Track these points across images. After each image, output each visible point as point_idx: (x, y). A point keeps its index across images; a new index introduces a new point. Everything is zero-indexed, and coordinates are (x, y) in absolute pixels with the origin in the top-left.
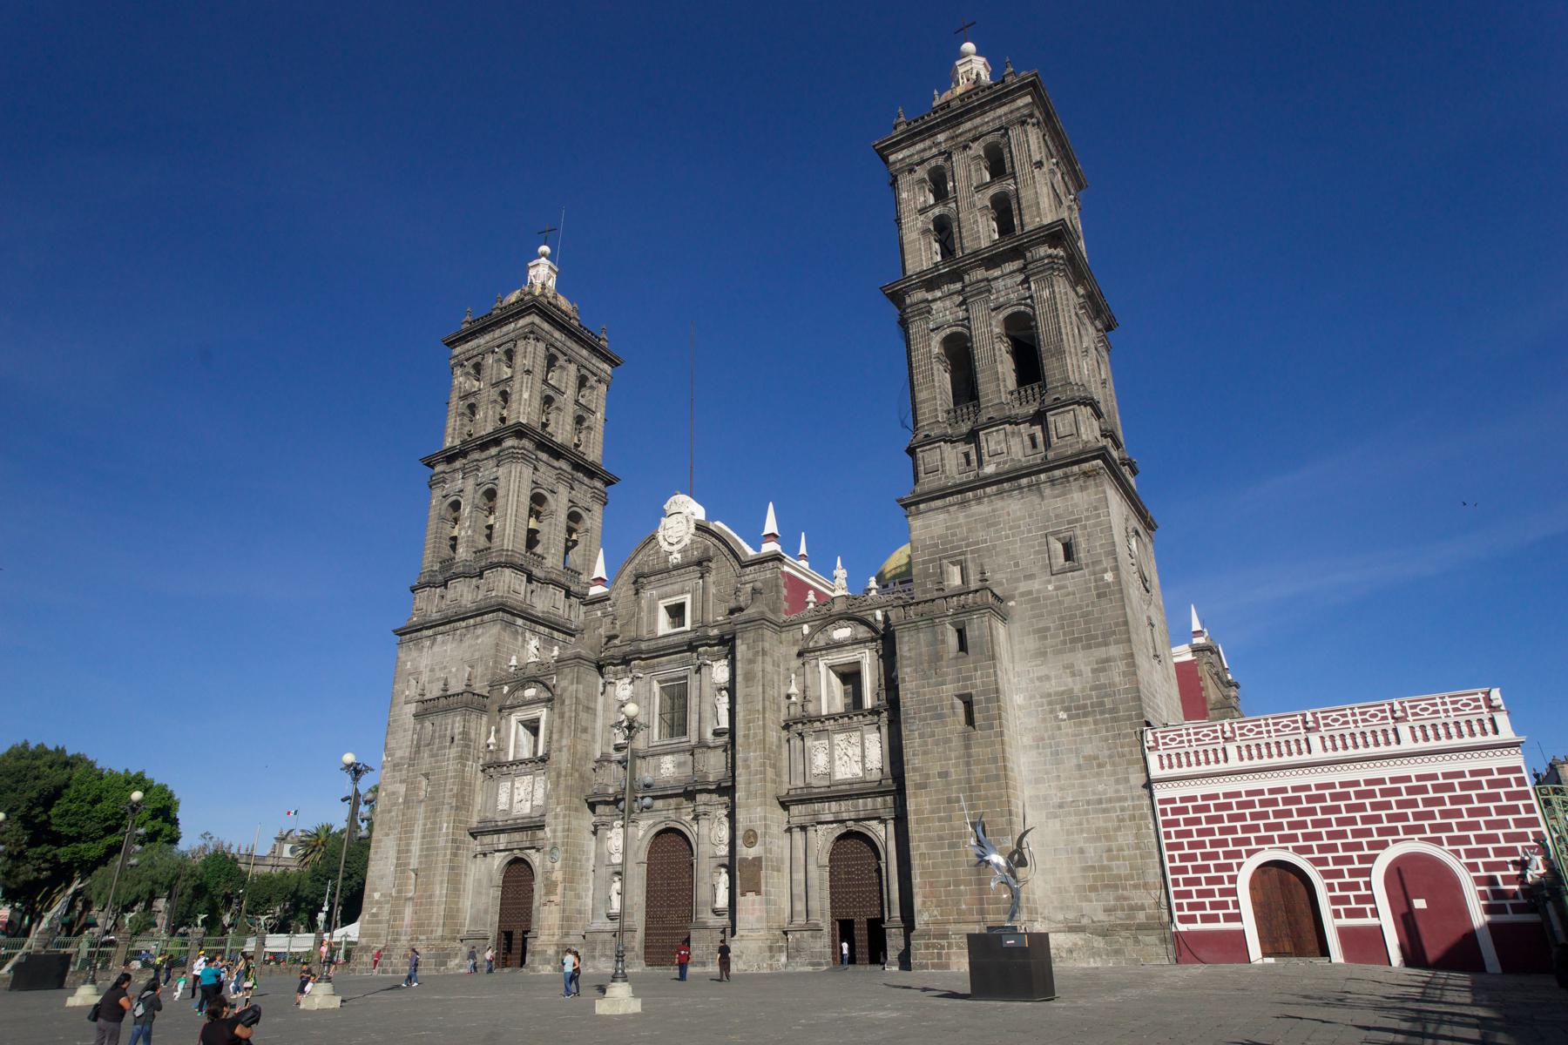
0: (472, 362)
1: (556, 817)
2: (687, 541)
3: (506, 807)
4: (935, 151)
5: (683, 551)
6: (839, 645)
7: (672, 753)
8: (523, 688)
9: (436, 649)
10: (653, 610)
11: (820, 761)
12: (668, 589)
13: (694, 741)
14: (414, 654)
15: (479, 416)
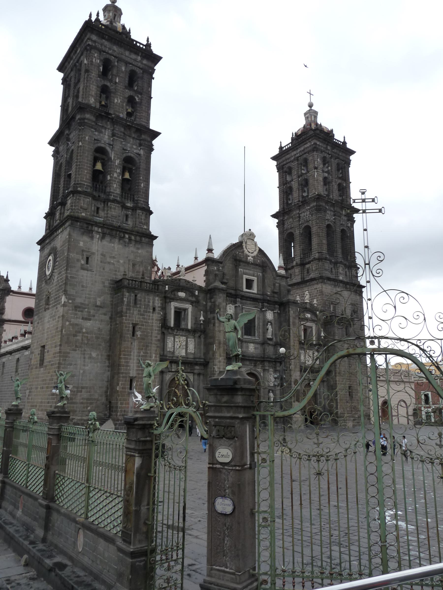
0: (108, 56)
1: (220, 362)
2: (255, 253)
3: (172, 350)
4: (327, 151)
5: (253, 257)
6: (307, 319)
7: (253, 343)
8: (179, 291)
9: (105, 242)
10: (242, 278)
11: (302, 357)
12: (247, 271)
13: (260, 339)
14: (86, 238)
15: (117, 100)
